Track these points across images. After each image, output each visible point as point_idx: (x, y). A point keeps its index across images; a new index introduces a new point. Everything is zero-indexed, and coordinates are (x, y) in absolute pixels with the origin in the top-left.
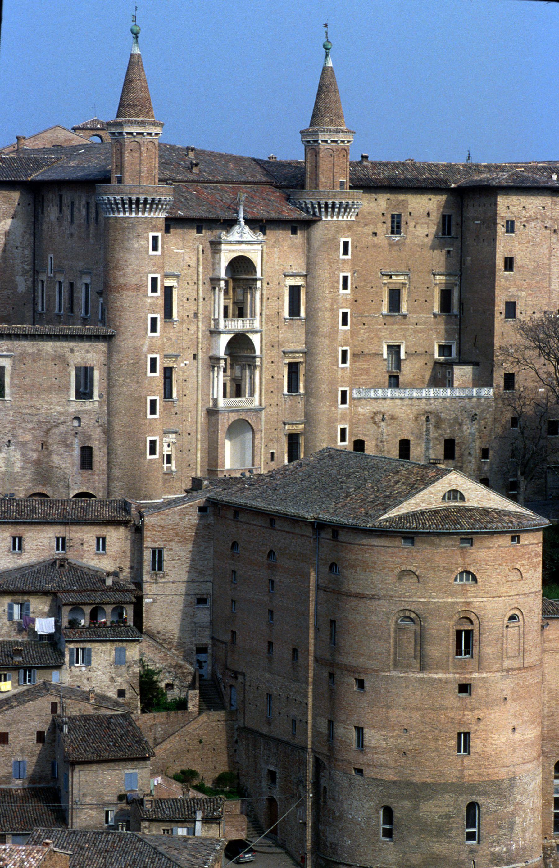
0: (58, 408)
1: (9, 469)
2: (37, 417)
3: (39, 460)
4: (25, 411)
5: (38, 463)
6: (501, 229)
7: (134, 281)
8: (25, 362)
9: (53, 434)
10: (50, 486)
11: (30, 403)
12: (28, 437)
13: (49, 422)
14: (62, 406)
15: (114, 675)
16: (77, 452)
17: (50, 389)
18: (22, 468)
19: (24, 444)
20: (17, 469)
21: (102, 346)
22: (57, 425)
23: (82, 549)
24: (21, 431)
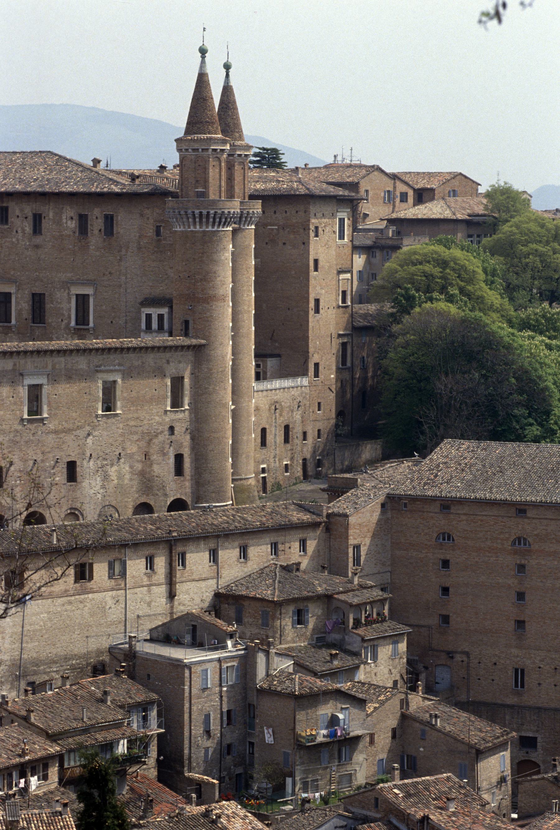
0: (157, 418)
1: (121, 482)
2: (141, 428)
3: (143, 471)
4: (132, 423)
5: (142, 474)
6: (312, 234)
7: (221, 292)
8: (132, 375)
9: (154, 443)
10: (153, 495)
11: (135, 415)
12: (135, 449)
13: (150, 433)
14: (160, 416)
15: (391, 668)
16: (172, 460)
17: (151, 400)
18: (131, 480)
19: (131, 456)
20: (126, 481)
21: (190, 355)
22: (156, 436)
23: (290, 552)
24: (129, 443)
